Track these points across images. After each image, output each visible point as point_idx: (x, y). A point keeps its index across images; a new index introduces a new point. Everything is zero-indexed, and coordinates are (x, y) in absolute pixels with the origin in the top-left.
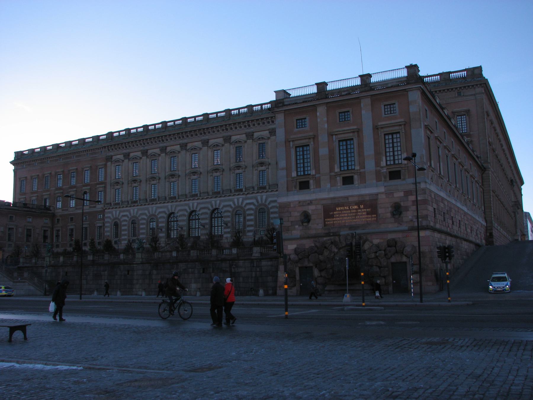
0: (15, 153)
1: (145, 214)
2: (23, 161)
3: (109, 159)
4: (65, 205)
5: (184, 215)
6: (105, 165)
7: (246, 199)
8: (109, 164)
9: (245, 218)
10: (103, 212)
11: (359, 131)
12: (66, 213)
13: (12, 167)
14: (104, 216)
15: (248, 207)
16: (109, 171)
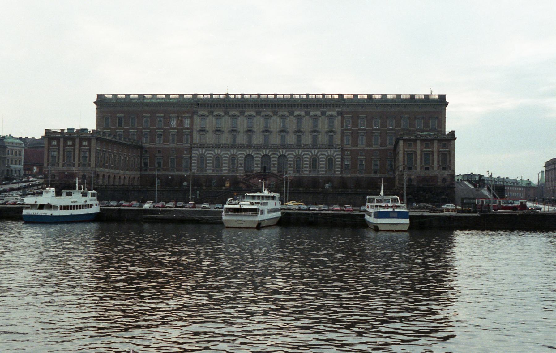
0: (98, 95)
1: (227, 154)
2: (102, 102)
3: (195, 113)
4: (153, 140)
5: (259, 157)
6: (191, 118)
7: (304, 151)
8: (195, 117)
9: (303, 163)
10: (190, 150)
11: (433, 152)
12: (154, 146)
13: (95, 106)
14: (190, 153)
15: (305, 156)
16: (195, 122)
